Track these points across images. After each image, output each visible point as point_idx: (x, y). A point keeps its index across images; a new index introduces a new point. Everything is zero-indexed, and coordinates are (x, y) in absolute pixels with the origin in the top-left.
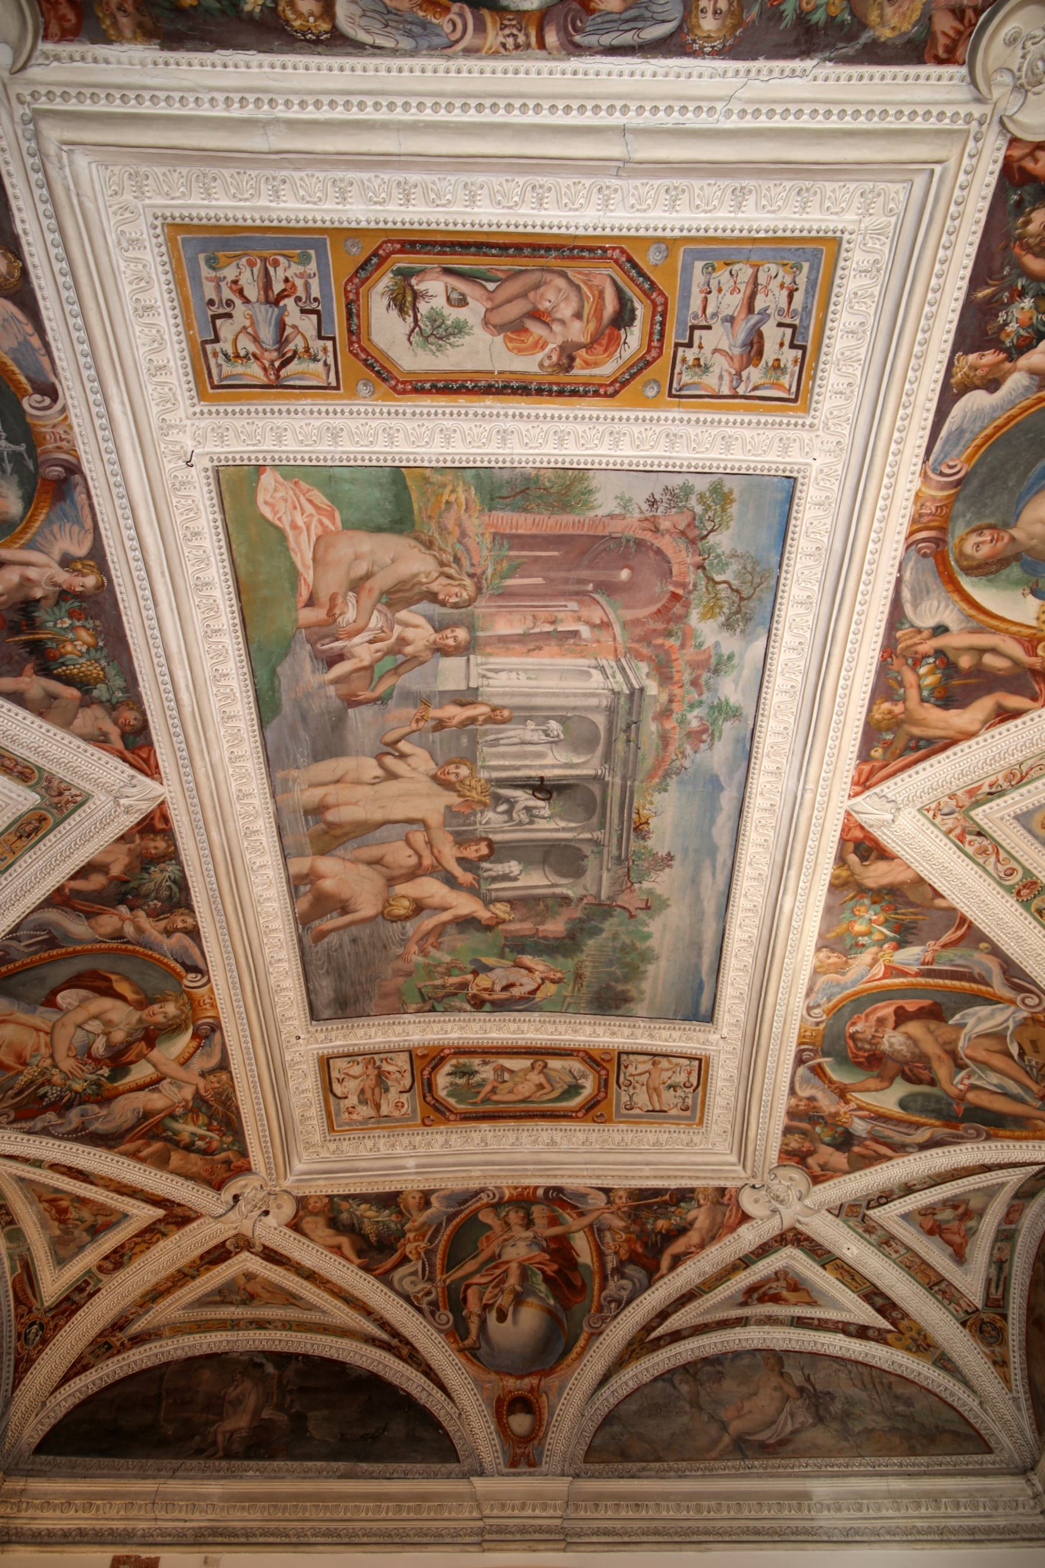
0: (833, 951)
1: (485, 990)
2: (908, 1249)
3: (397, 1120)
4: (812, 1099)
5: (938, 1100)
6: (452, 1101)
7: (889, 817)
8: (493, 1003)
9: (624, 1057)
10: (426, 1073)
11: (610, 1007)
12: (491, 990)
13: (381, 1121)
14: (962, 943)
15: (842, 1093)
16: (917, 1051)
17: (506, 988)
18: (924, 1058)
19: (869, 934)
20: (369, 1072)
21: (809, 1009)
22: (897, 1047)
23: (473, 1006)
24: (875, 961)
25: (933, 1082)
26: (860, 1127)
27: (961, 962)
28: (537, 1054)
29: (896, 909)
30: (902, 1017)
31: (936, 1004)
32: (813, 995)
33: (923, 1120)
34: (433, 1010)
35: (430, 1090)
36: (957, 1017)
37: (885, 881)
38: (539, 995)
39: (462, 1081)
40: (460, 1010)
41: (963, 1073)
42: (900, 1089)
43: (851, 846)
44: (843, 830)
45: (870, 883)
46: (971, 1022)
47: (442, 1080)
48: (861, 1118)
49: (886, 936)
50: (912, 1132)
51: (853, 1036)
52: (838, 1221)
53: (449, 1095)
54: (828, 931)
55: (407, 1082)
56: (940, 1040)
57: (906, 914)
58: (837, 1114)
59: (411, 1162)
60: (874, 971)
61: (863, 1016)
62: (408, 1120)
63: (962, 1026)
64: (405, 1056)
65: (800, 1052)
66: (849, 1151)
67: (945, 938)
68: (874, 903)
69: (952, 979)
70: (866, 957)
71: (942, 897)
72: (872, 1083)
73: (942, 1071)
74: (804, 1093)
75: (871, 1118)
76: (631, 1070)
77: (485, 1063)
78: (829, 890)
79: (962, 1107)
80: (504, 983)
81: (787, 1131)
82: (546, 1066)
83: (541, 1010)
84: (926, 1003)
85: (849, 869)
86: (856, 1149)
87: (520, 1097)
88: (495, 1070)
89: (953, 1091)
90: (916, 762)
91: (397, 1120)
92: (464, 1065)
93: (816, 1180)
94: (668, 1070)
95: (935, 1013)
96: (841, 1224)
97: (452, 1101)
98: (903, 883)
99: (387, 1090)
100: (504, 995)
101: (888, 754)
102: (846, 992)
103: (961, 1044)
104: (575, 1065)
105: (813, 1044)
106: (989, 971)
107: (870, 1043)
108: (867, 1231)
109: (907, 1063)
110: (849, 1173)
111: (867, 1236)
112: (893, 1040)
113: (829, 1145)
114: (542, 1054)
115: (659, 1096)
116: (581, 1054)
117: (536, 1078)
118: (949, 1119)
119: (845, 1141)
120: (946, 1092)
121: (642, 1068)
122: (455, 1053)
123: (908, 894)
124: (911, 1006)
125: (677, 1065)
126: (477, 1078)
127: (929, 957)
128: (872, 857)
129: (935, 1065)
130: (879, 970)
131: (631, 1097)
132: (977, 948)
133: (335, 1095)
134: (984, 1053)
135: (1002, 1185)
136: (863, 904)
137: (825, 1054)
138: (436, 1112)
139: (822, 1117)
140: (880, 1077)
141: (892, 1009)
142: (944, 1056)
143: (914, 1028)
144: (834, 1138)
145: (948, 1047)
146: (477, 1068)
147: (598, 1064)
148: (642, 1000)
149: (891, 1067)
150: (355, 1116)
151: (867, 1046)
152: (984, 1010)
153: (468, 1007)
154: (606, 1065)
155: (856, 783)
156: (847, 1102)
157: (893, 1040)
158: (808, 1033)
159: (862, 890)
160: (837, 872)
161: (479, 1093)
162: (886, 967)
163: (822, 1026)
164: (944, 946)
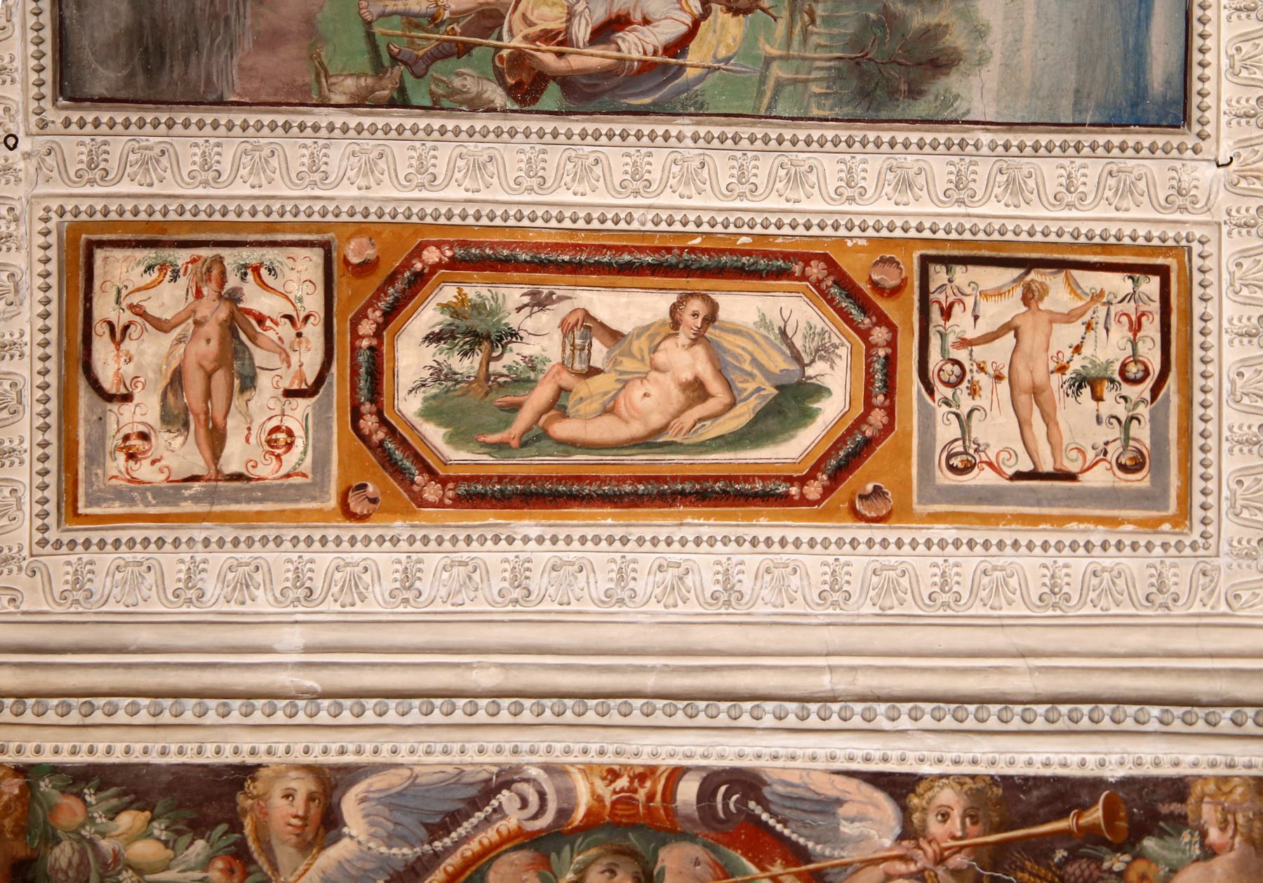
1: (548, 36)
3: (269, 492)
6: (434, 434)
8: (568, 83)
9: (939, 275)
10: (367, 328)
11: (893, 93)
12: (559, 39)
13: (222, 494)
17: (605, 32)
20: (204, 310)
23: (511, 91)
28: (687, 271)
34: (400, 101)
35: (375, 393)
38: (696, 55)
39: (467, 366)
40: (477, 105)
47: (412, 357)
53: (430, 413)
55: (309, 359)
59: (295, 637)
62: (300, 492)
64: (308, 264)
76: (962, 323)
77: (540, 303)
80: (600, 15)
82: (711, 318)
83: (700, 112)
87: (636, 429)
88: (567, 328)
91: (269, 492)
92: (478, 308)
94: (1069, 318)
97: (434, 434)
99: (249, 383)
100: (592, 59)
104: (796, 310)
114: (705, 272)
115: (1049, 419)
116: (816, 270)
117: (685, 360)
121: (996, 312)
122: (454, 264)
125: (1097, 297)
126: (512, 357)
131: (965, 423)
133: (95, 384)
138: (388, 471)
146: (514, 320)
147: (866, 307)
148: (982, 61)
150: (144, 471)
153: (497, 95)
154: (886, 295)
161: (515, 408)
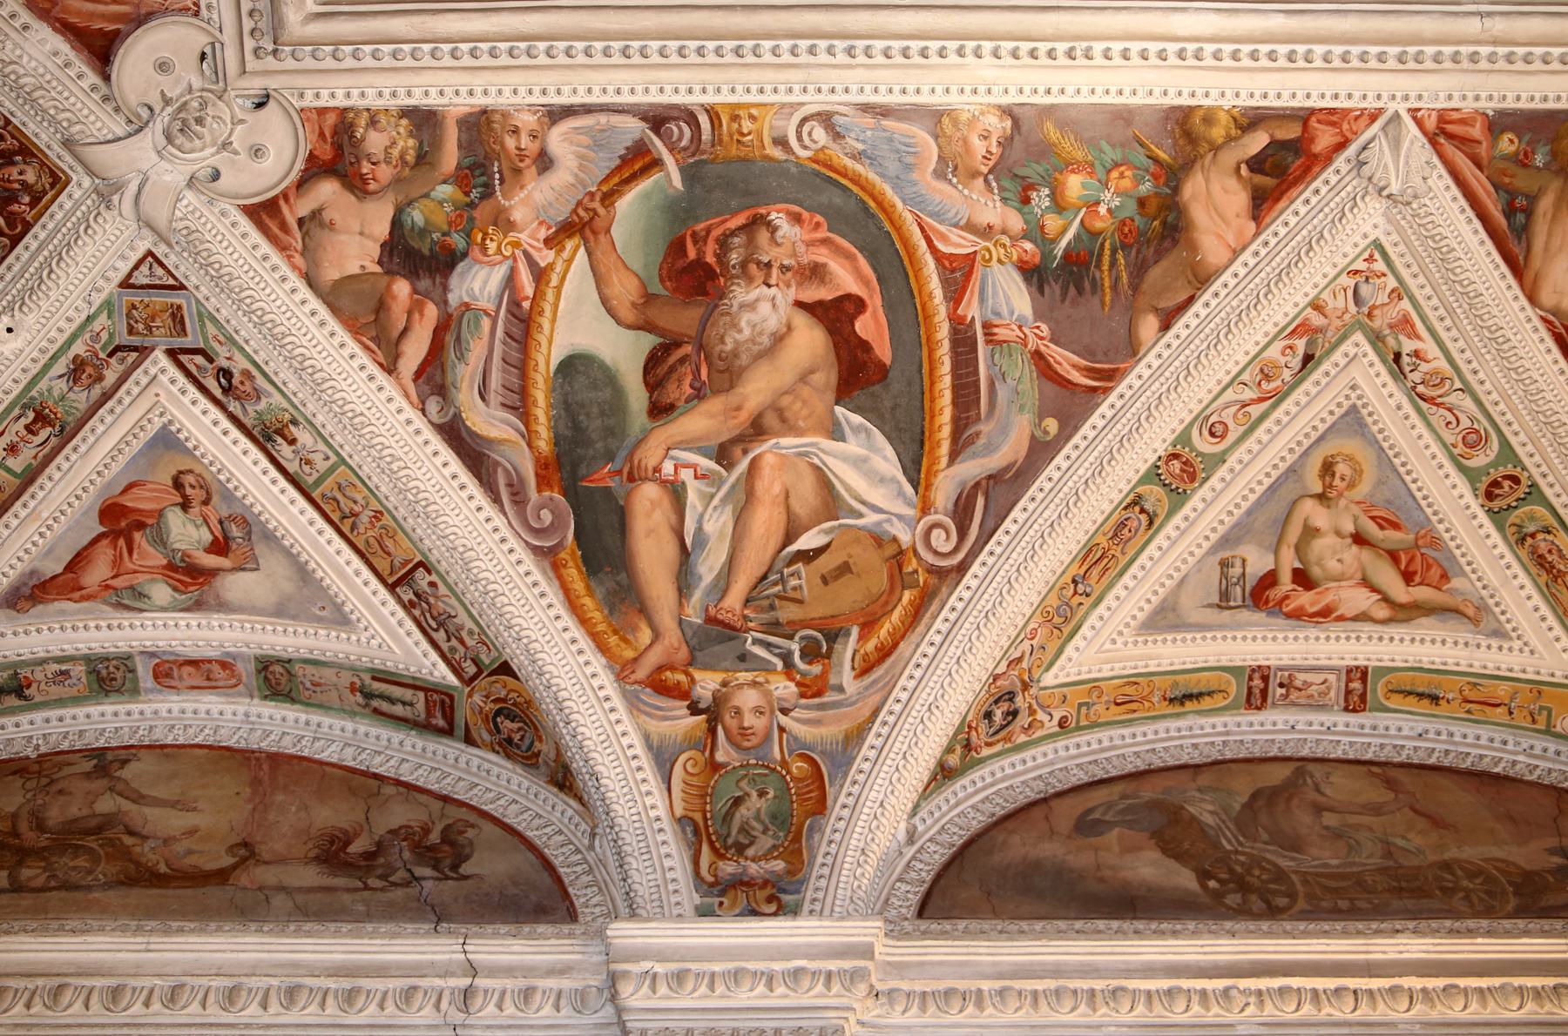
0: (1006, 143)
2: (29, 477)
4: (544, 162)
5: (616, 431)
7: (1394, 188)
14: (1050, 388)
15: (579, 226)
16: (744, 359)
18: (727, 375)
19: (1059, 205)
21: (826, 119)
22: (745, 320)
24: (986, 232)
25: (660, 410)
26: (479, 284)
27: (1002, 393)
29: (1124, 246)
30: (836, 315)
31: (883, 372)
32: (869, 120)
33: (541, 413)
36: (857, 419)
37: (1199, 214)
41: (707, 464)
42: (623, 352)
43: (1291, 132)
44: (1332, 111)
45: (1193, 188)
46: (852, 447)
48: (511, 280)
49: (1055, 241)
50: (494, 399)
51: (758, 222)
52: (110, 288)
54: (1062, 125)
56: (785, 401)
57: (1111, 271)
58: (510, 226)
60: (954, 235)
61: (823, 233)
63: (836, 432)
65: (690, 117)
66: (388, 272)
67: (1056, 353)
68: (1142, 203)
69: (956, 389)
70: (993, 211)
71: (1166, 326)
72: (625, 290)
73: (702, 421)
74: (558, 140)
75: (515, 303)
78: (1174, 109)
79: (612, 483)
81: (424, 120)
84: (884, 352)
85: (1230, 139)
86: (402, 288)
89: (650, 455)
90: (1483, 217)
93: (264, 213)
95: (856, 374)
96: (98, 299)
98: (1193, 247)
101: (1502, 165)
102: (888, 190)
103: (786, 441)
105: (717, 140)
106: (990, 449)
107: (744, 265)
108: (78, 366)
109: (701, 347)
110: (311, 284)
111: (61, 367)
112: (761, 309)
113: (396, 223)
118: (566, 466)
119: (419, 258)
120: (640, 442)
123: (1164, 263)
124: (870, 326)
127: (1002, 333)
128: (1260, 179)
129: (715, 404)
130: (958, 244)
132: (1041, 418)
134: (777, 489)
135: (341, 619)
136: (1138, 181)
137: (691, 174)
139: (488, 193)
140: (649, 298)
141: (854, 287)
142: (744, 416)
143: (810, 340)
144: (424, 232)
145: (771, 420)
149: (684, 319)
151: (734, 258)
152: (887, 461)
155: (1443, 117)
156: (548, 242)
157: (764, 308)
158: (747, 125)
159: (1172, 175)
160: (1224, 118)
162: (971, 258)
163: (777, 153)
164: (1038, 356)
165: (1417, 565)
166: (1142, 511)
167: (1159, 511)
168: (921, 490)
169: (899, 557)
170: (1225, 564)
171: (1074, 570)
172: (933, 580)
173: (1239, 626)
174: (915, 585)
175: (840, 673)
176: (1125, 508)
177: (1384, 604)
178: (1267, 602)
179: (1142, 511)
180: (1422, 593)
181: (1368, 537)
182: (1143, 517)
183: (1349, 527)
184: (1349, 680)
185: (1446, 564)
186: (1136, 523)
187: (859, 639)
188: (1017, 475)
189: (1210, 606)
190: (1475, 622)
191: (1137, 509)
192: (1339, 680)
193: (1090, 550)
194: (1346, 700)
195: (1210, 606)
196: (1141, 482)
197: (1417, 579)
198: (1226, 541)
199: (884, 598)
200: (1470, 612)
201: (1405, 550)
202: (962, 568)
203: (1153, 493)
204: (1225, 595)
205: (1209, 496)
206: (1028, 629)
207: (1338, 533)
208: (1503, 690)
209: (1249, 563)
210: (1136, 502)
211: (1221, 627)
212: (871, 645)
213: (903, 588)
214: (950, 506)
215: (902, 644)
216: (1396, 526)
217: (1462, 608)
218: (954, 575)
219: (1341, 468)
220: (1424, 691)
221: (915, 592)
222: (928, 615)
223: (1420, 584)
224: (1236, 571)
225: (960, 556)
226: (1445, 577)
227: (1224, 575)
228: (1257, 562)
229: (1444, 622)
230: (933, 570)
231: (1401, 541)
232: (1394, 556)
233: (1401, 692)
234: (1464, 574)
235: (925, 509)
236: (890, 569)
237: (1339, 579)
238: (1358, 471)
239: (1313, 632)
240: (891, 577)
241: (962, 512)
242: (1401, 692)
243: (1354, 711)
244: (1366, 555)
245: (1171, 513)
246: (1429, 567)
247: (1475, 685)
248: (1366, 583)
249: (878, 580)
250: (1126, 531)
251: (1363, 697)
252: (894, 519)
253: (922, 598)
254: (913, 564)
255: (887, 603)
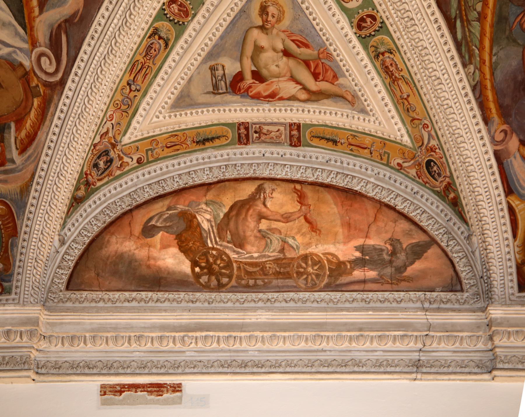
165: (320, 69)
166: (160, 38)
167: (170, 37)
168: (28, 30)
169: (26, 76)
170: (213, 69)
171: (127, 78)
172: (48, 92)
173: (227, 103)
174: (38, 95)
175: (11, 151)
176: (149, 37)
177: (304, 91)
178: (240, 90)
179: (160, 38)
180: (324, 86)
181: (292, 52)
182: (161, 42)
183: (280, 47)
184: (291, 130)
185: (335, 69)
186: (157, 46)
187: (17, 130)
188: (82, 19)
189: (208, 93)
190: (352, 104)
191: (157, 37)
192: (285, 129)
193: (134, 65)
194: (291, 140)
195: (208, 93)
196: (156, 20)
197: (321, 77)
198: (211, 55)
199: (23, 104)
200: (350, 98)
201: (314, 60)
202: (62, 83)
203: (164, 26)
204: (216, 87)
205: (198, 27)
206: (108, 116)
207: (274, 50)
208: (368, 141)
209: (226, 67)
210: (155, 32)
211: (216, 104)
212: (23, 134)
213: (33, 98)
214: (47, 41)
215: (39, 133)
216: (307, 46)
217: (345, 95)
218: (59, 87)
219: (272, 10)
220: (329, 138)
221: (40, 99)
222: (50, 114)
223: (323, 80)
224: (220, 72)
225: (60, 75)
226: (335, 77)
227: (213, 75)
228: (231, 67)
229: (336, 102)
230: (46, 85)
231: (310, 55)
232: (307, 63)
233: (318, 137)
234: (345, 76)
235: (34, 43)
236: (23, 85)
237: (278, 76)
238: (282, 12)
239: (267, 106)
240: (25, 90)
241: (55, 44)
242: (318, 137)
243: (295, 146)
244: (292, 63)
245: (178, 38)
246: (327, 71)
247: (355, 136)
248: (293, 79)
249: (19, 92)
250: (152, 51)
251: (299, 139)
252: (18, 51)
253: (44, 103)
254: (34, 83)
255: (26, 107)
